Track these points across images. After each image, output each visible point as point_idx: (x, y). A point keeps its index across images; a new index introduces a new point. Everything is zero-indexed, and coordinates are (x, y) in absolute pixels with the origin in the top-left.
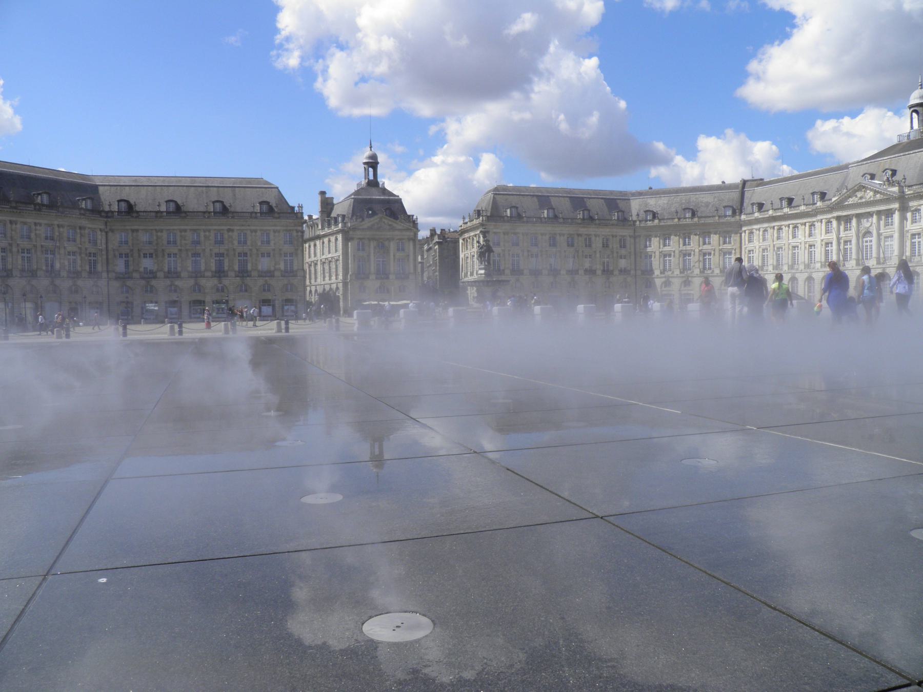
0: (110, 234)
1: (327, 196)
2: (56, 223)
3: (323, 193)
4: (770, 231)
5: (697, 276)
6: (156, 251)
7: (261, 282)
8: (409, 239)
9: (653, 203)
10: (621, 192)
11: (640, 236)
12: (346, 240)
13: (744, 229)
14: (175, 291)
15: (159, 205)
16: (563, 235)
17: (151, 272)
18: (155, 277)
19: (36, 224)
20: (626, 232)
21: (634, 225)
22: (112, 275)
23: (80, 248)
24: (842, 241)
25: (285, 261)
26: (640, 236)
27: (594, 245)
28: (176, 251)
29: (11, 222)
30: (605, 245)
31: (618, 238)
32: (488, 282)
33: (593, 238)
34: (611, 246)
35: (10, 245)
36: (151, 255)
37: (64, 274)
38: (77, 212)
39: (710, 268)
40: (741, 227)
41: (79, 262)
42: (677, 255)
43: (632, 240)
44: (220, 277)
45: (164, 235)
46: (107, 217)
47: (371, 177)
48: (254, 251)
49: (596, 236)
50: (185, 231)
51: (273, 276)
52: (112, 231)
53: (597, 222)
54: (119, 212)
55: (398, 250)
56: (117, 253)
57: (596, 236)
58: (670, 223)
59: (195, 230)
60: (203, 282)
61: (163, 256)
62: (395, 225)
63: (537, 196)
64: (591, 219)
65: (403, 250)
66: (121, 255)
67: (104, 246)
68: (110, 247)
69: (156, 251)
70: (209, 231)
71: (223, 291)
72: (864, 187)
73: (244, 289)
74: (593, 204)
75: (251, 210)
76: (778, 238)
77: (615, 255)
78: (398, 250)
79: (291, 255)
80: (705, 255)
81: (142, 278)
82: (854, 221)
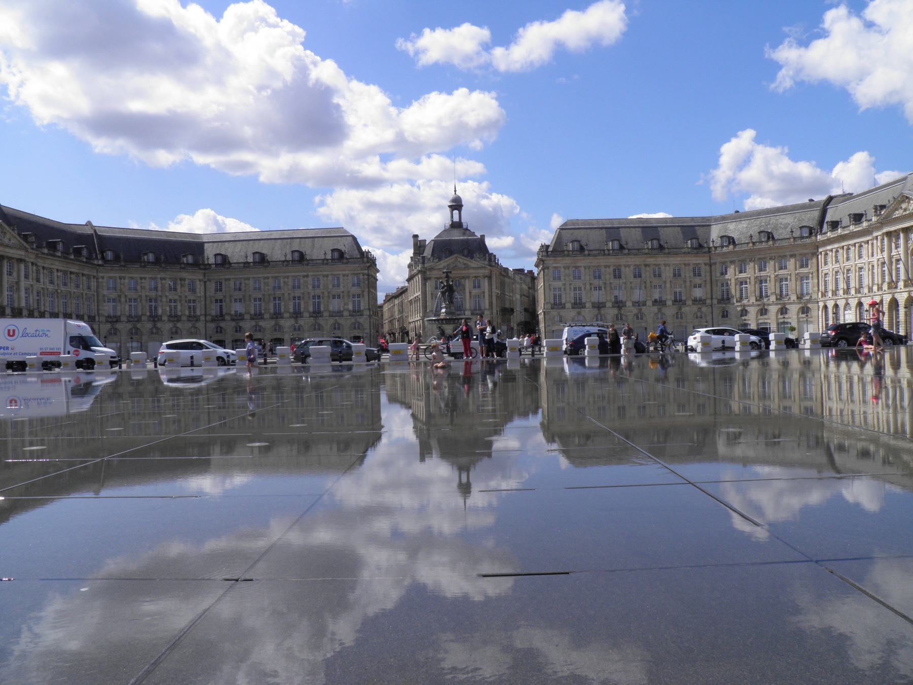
0: (208, 283)
1: (420, 239)
2: (159, 276)
4: (841, 251)
5: (773, 304)
6: (244, 296)
7: (331, 321)
8: (485, 277)
9: (735, 230)
10: (703, 218)
11: (715, 264)
12: (425, 279)
13: (820, 250)
14: (260, 331)
15: (285, 256)
16: (629, 266)
17: (241, 315)
18: (243, 319)
19: (141, 278)
20: (700, 260)
21: (709, 252)
22: (209, 318)
23: (180, 297)
24: (894, 260)
25: (354, 302)
26: (715, 264)
27: (663, 276)
28: (260, 296)
29: (120, 278)
30: (638, 275)
31: (691, 267)
32: (450, 319)
33: (663, 268)
34: (683, 275)
35: (120, 296)
36: (240, 300)
37: (165, 318)
38: (178, 267)
39: (807, 294)
40: (818, 248)
41: (179, 308)
42: (753, 283)
43: (708, 268)
44: (154, 321)
45: (251, 282)
46: (205, 269)
47: (456, 219)
48: (326, 294)
49: (665, 265)
50: (268, 278)
51: (342, 316)
52: (209, 280)
53: (667, 251)
54: (254, 262)
55: (475, 287)
56: (213, 299)
57: (665, 265)
58: (744, 248)
59: (276, 277)
60: (282, 322)
61: (250, 300)
62: (469, 264)
63: (606, 228)
64: (661, 247)
65: (479, 287)
66: (216, 301)
67: (203, 294)
68: (208, 294)
69: (244, 296)
70: (288, 277)
71: (299, 329)
72: (907, 198)
73: (317, 328)
74: (667, 236)
75: (283, 259)
76: (848, 259)
77: (688, 284)
78: (475, 287)
79: (359, 296)
80: (781, 280)
81: (233, 320)
82: (902, 235)
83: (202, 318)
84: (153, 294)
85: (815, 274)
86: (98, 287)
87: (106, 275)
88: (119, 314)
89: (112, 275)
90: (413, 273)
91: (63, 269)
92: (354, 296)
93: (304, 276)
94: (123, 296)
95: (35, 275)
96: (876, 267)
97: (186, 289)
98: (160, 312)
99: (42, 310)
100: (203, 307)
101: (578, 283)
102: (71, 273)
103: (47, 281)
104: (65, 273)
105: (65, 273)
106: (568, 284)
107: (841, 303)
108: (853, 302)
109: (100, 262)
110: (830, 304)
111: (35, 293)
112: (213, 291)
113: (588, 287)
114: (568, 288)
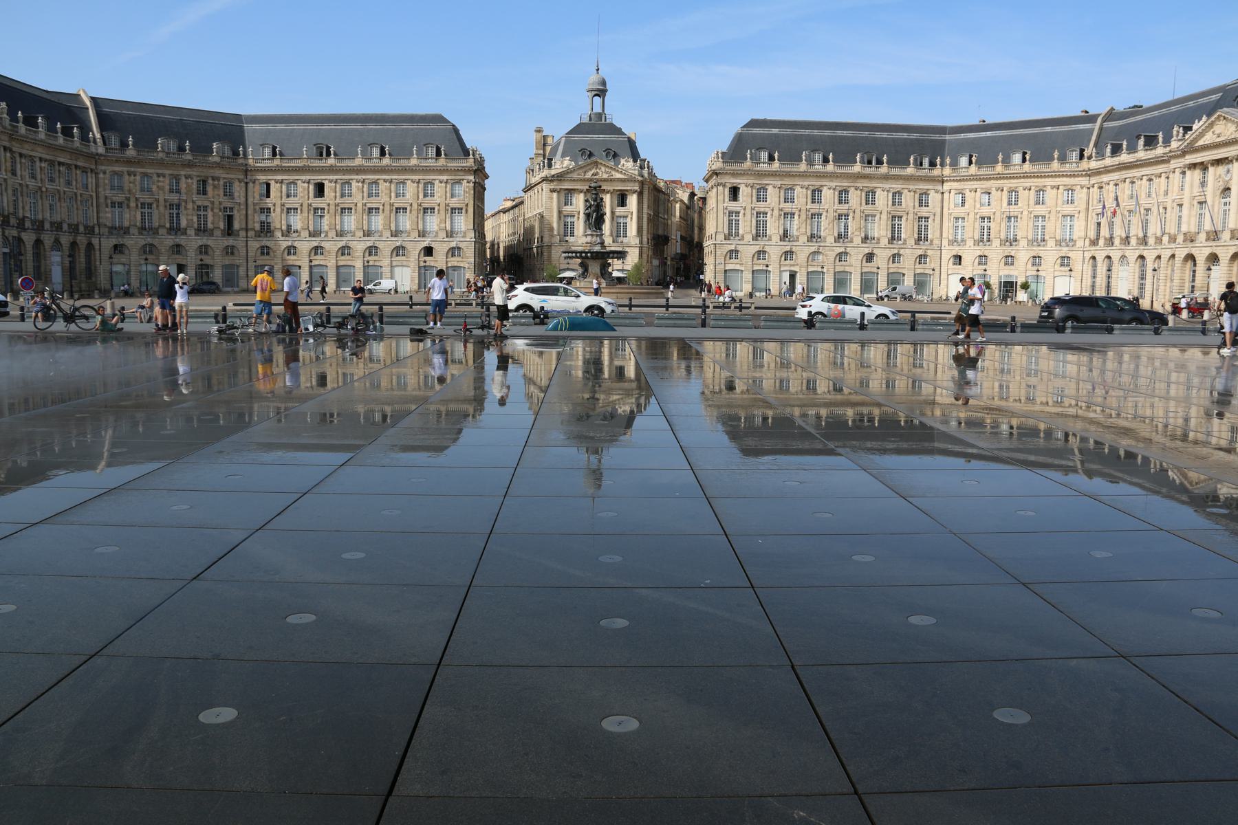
0: (251, 185)
3: (539, 131)
19: (158, 175)
23: (213, 203)
35: (128, 199)
41: (210, 218)
43: (939, 196)
48: (415, 206)
67: (243, 200)
68: (250, 200)
73: (399, 251)
83: (243, 233)
84: (174, 198)
85: (1083, 215)
86: (97, 186)
87: (109, 169)
88: (126, 224)
89: (117, 169)
90: (533, 181)
91: (48, 157)
92: (453, 209)
93: (385, 181)
94: (132, 200)
95: (9, 164)
96: (1169, 210)
97: (221, 192)
98: (184, 223)
99: (21, 215)
100: (243, 217)
101: (761, 206)
102: (60, 163)
103: (26, 174)
104: (51, 163)
105: (51, 163)
106: (748, 208)
107: (1116, 255)
108: (1132, 255)
109: (101, 150)
110: (1100, 256)
111: (10, 192)
112: (257, 197)
113: (776, 212)
114: (748, 212)
